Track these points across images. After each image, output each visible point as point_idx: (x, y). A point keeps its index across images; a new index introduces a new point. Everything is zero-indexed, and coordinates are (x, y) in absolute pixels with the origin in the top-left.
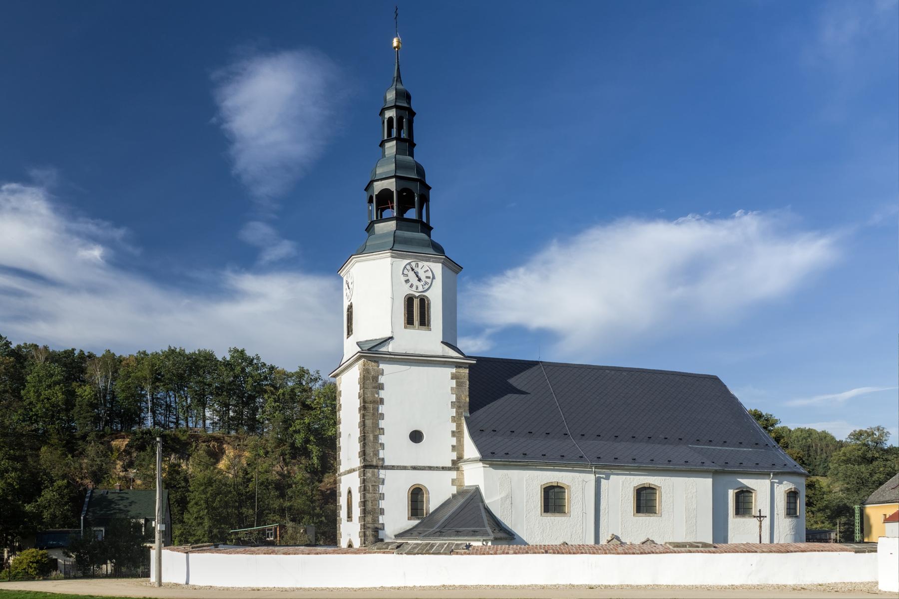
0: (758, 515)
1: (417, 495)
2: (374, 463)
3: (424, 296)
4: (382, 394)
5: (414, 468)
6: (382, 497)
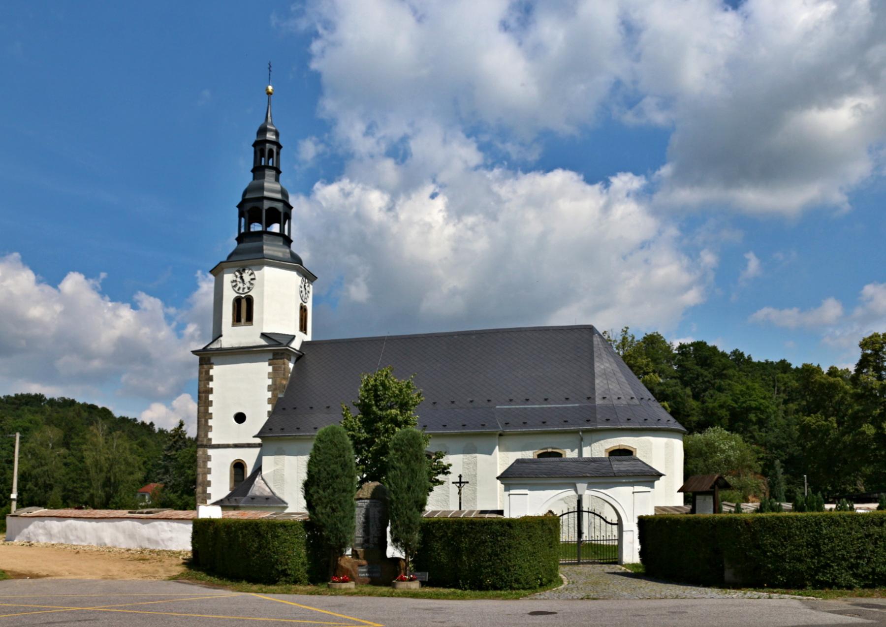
2: (205, 443)
3: (249, 296)
6: (209, 471)
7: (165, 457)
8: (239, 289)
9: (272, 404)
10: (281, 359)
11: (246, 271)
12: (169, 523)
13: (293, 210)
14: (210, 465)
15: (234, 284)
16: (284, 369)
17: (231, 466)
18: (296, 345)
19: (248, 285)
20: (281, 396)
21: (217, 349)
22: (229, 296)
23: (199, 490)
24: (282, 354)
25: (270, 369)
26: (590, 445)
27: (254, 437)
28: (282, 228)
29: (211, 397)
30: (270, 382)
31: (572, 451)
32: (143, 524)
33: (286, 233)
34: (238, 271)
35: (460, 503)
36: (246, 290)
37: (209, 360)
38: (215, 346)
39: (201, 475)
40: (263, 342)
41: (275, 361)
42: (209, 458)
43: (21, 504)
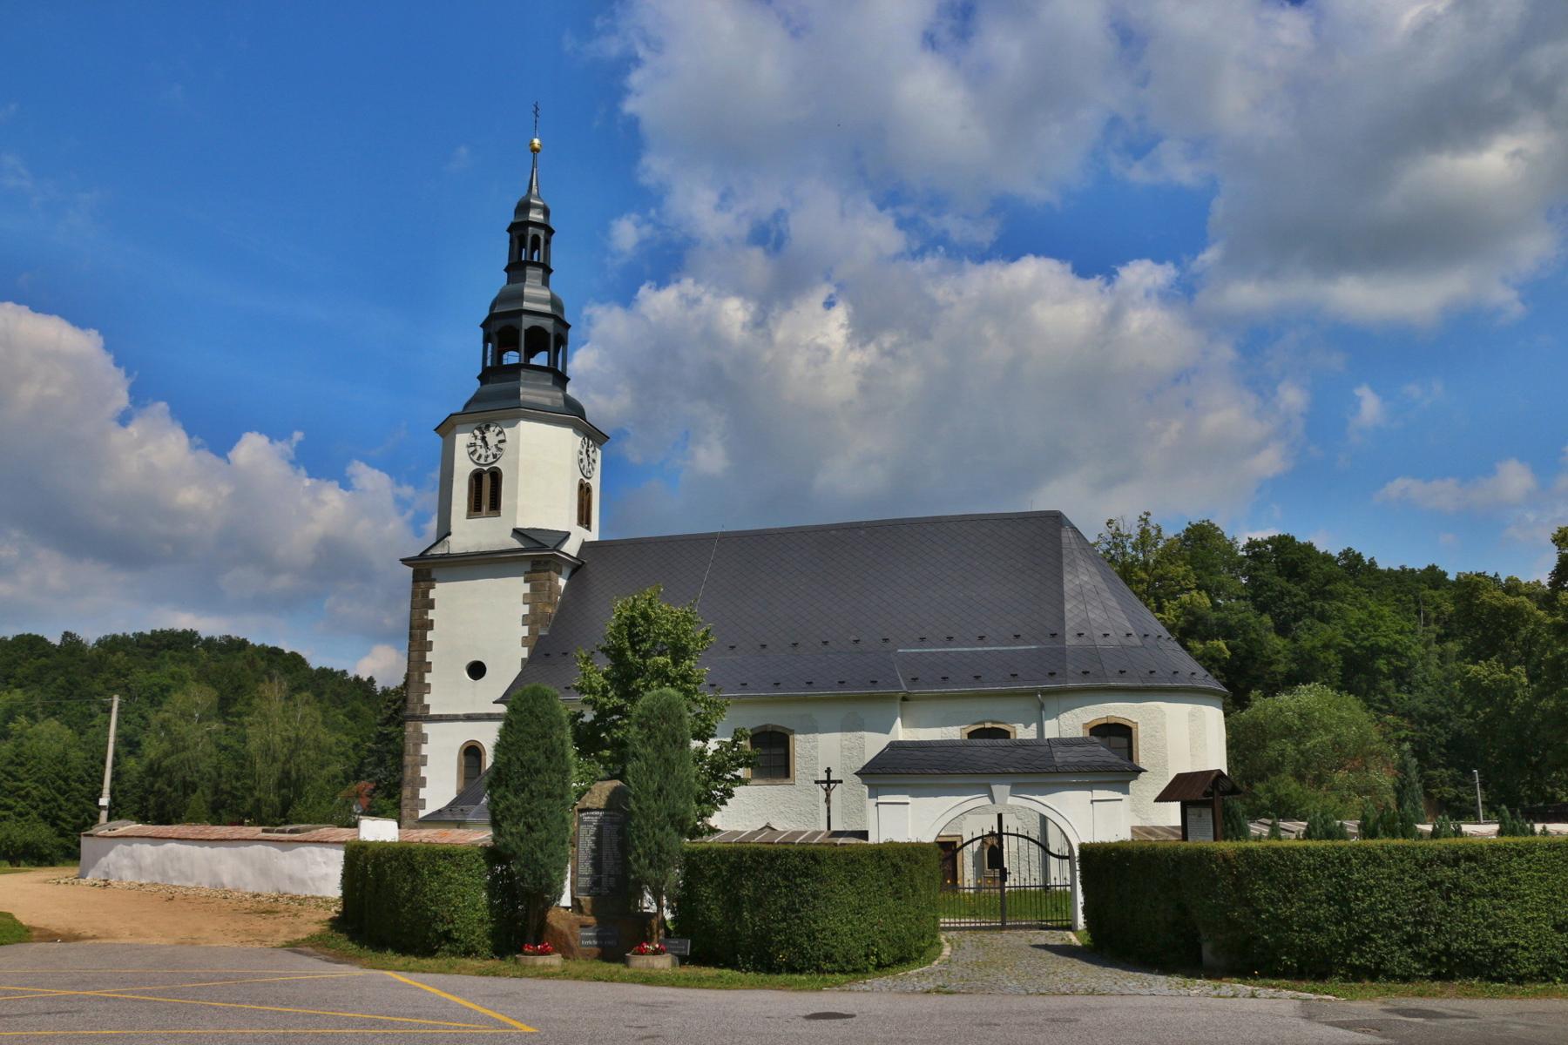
0: (825, 779)
1: (472, 752)
2: (418, 712)
3: (496, 468)
4: (431, 615)
5: (469, 718)
7: (378, 737)
8: (480, 456)
9: (529, 647)
10: (545, 571)
11: (492, 429)
12: (324, 849)
13: (570, 332)
14: (425, 750)
15: (472, 449)
16: (550, 588)
17: (460, 752)
18: (571, 548)
19: (494, 450)
20: (543, 633)
21: (442, 556)
22: (464, 467)
23: (406, 792)
24: (547, 563)
25: (527, 588)
26: (1057, 716)
27: (494, 703)
28: (553, 359)
29: (430, 636)
30: (526, 610)
31: (1026, 727)
32: (283, 851)
33: (560, 369)
34: (479, 429)
35: (829, 818)
36: (491, 459)
37: (429, 573)
38: (438, 551)
39: (410, 768)
40: (516, 544)
41: (535, 575)
42: (423, 739)
43: (115, 813)
